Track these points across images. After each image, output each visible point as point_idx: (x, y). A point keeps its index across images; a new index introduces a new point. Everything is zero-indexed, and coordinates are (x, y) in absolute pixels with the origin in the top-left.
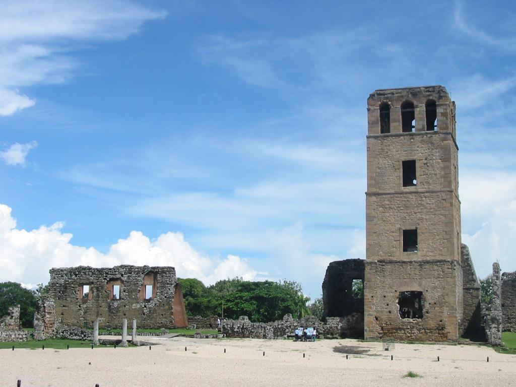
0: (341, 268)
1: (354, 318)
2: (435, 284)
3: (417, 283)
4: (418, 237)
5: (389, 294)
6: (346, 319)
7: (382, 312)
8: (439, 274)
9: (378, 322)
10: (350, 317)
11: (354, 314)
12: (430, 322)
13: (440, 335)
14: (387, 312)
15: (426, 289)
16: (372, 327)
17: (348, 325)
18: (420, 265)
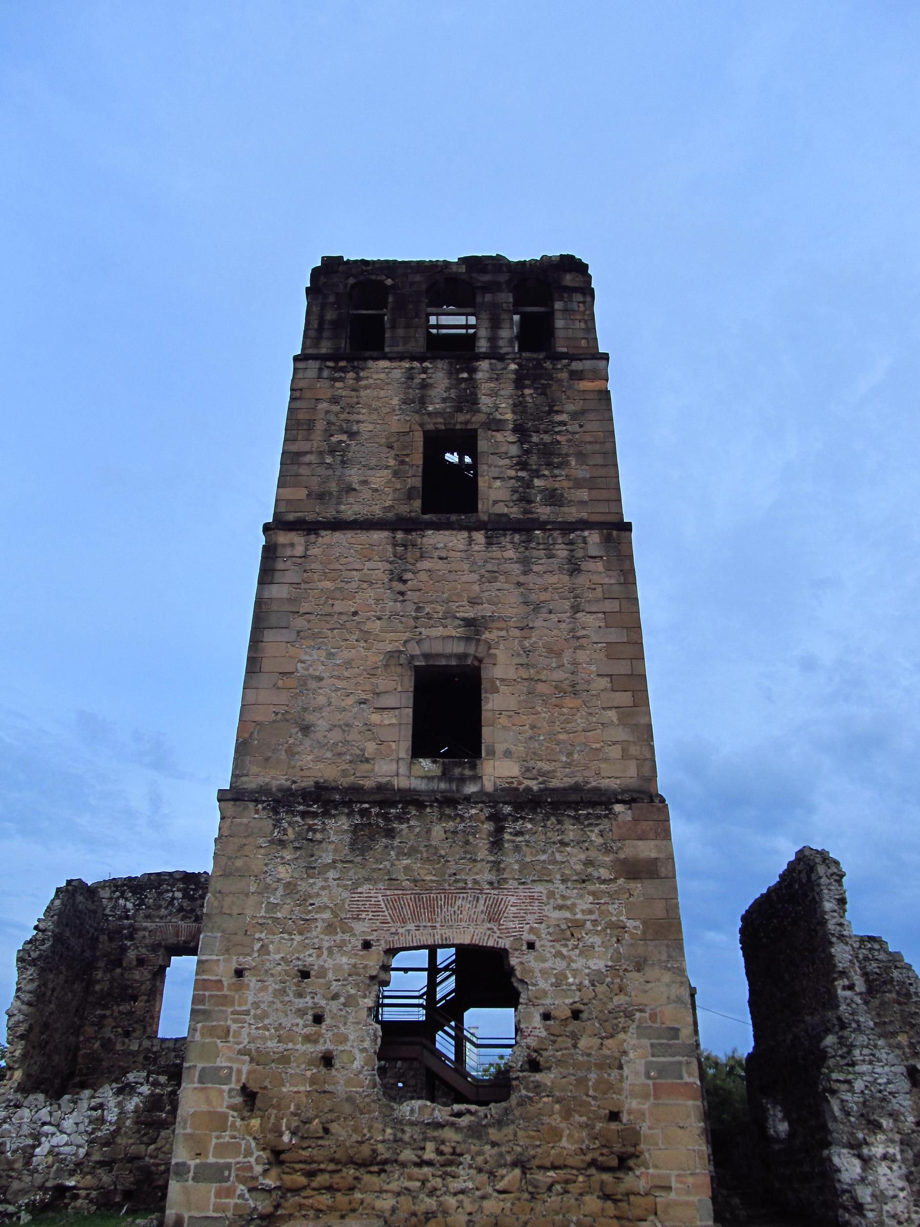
0: (129, 905)
1: (132, 1103)
2: (571, 908)
3: (481, 907)
4: (483, 695)
5: (329, 964)
6: (84, 1105)
7: (284, 1059)
8: (588, 863)
9: (255, 1123)
10: (107, 1093)
11: (131, 1077)
12: (556, 1120)
13: (609, 1204)
14: (310, 1063)
15: (527, 937)
16: (221, 1149)
17: (90, 1142)
18: (497, 819)
